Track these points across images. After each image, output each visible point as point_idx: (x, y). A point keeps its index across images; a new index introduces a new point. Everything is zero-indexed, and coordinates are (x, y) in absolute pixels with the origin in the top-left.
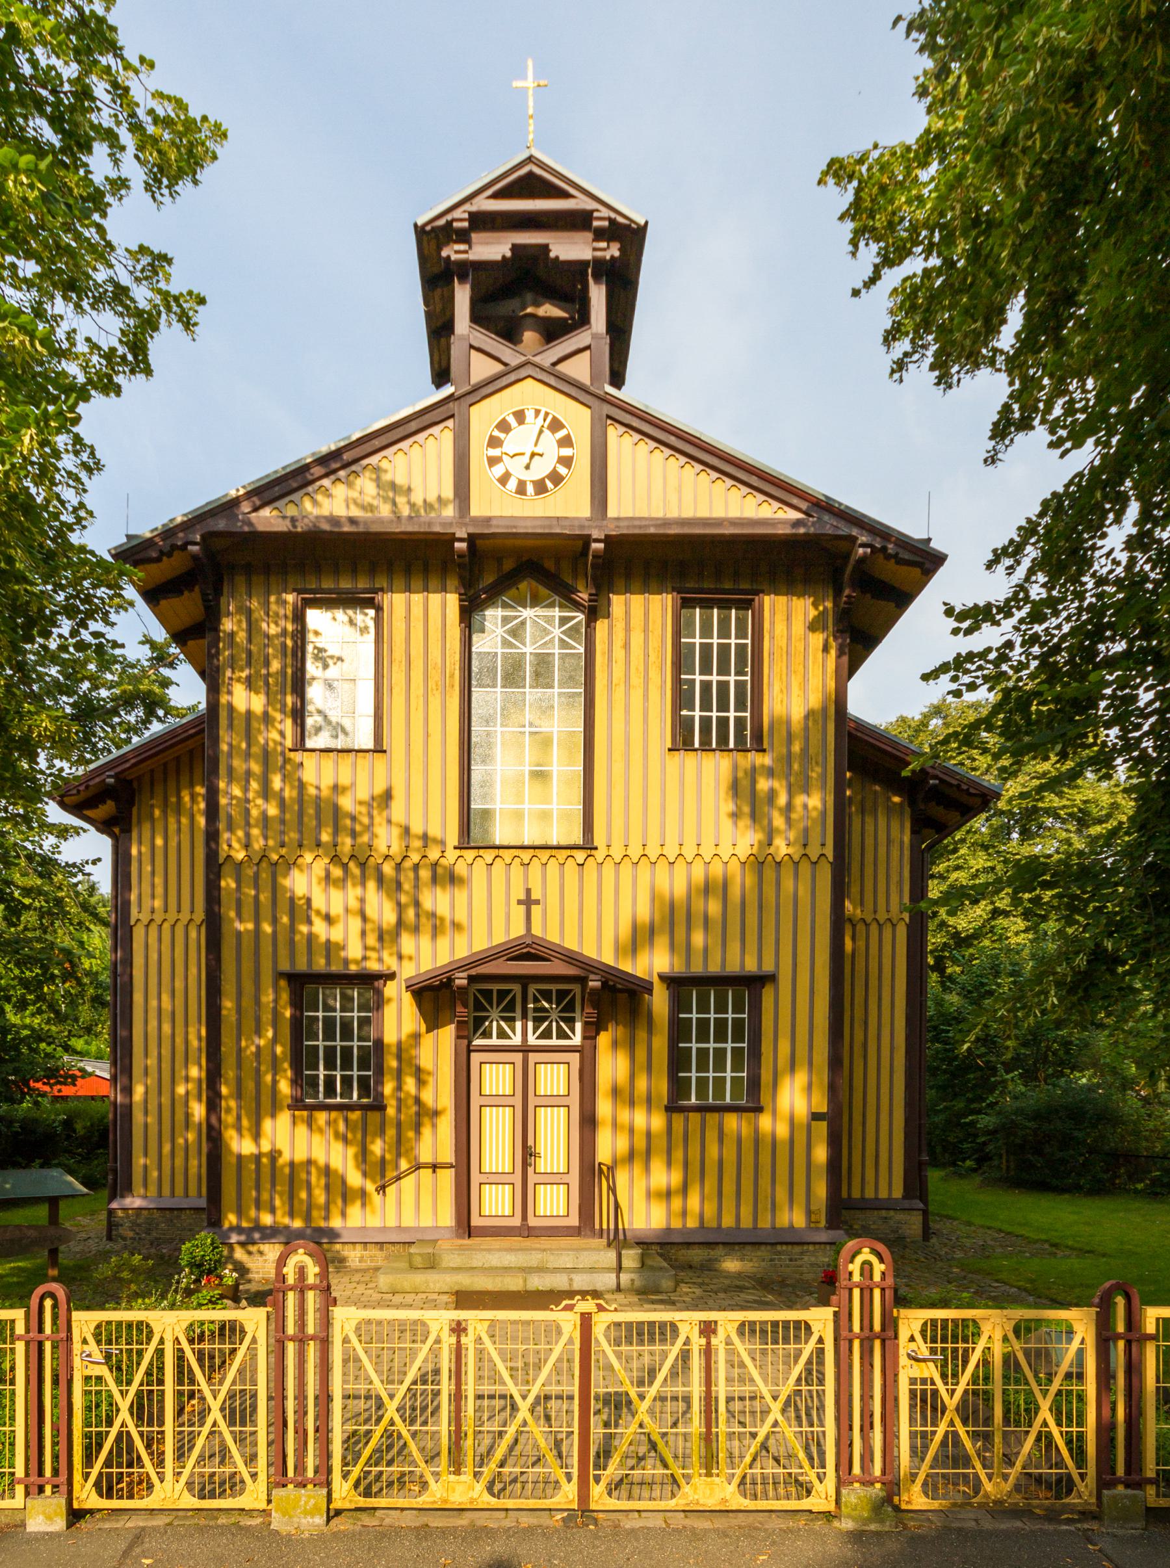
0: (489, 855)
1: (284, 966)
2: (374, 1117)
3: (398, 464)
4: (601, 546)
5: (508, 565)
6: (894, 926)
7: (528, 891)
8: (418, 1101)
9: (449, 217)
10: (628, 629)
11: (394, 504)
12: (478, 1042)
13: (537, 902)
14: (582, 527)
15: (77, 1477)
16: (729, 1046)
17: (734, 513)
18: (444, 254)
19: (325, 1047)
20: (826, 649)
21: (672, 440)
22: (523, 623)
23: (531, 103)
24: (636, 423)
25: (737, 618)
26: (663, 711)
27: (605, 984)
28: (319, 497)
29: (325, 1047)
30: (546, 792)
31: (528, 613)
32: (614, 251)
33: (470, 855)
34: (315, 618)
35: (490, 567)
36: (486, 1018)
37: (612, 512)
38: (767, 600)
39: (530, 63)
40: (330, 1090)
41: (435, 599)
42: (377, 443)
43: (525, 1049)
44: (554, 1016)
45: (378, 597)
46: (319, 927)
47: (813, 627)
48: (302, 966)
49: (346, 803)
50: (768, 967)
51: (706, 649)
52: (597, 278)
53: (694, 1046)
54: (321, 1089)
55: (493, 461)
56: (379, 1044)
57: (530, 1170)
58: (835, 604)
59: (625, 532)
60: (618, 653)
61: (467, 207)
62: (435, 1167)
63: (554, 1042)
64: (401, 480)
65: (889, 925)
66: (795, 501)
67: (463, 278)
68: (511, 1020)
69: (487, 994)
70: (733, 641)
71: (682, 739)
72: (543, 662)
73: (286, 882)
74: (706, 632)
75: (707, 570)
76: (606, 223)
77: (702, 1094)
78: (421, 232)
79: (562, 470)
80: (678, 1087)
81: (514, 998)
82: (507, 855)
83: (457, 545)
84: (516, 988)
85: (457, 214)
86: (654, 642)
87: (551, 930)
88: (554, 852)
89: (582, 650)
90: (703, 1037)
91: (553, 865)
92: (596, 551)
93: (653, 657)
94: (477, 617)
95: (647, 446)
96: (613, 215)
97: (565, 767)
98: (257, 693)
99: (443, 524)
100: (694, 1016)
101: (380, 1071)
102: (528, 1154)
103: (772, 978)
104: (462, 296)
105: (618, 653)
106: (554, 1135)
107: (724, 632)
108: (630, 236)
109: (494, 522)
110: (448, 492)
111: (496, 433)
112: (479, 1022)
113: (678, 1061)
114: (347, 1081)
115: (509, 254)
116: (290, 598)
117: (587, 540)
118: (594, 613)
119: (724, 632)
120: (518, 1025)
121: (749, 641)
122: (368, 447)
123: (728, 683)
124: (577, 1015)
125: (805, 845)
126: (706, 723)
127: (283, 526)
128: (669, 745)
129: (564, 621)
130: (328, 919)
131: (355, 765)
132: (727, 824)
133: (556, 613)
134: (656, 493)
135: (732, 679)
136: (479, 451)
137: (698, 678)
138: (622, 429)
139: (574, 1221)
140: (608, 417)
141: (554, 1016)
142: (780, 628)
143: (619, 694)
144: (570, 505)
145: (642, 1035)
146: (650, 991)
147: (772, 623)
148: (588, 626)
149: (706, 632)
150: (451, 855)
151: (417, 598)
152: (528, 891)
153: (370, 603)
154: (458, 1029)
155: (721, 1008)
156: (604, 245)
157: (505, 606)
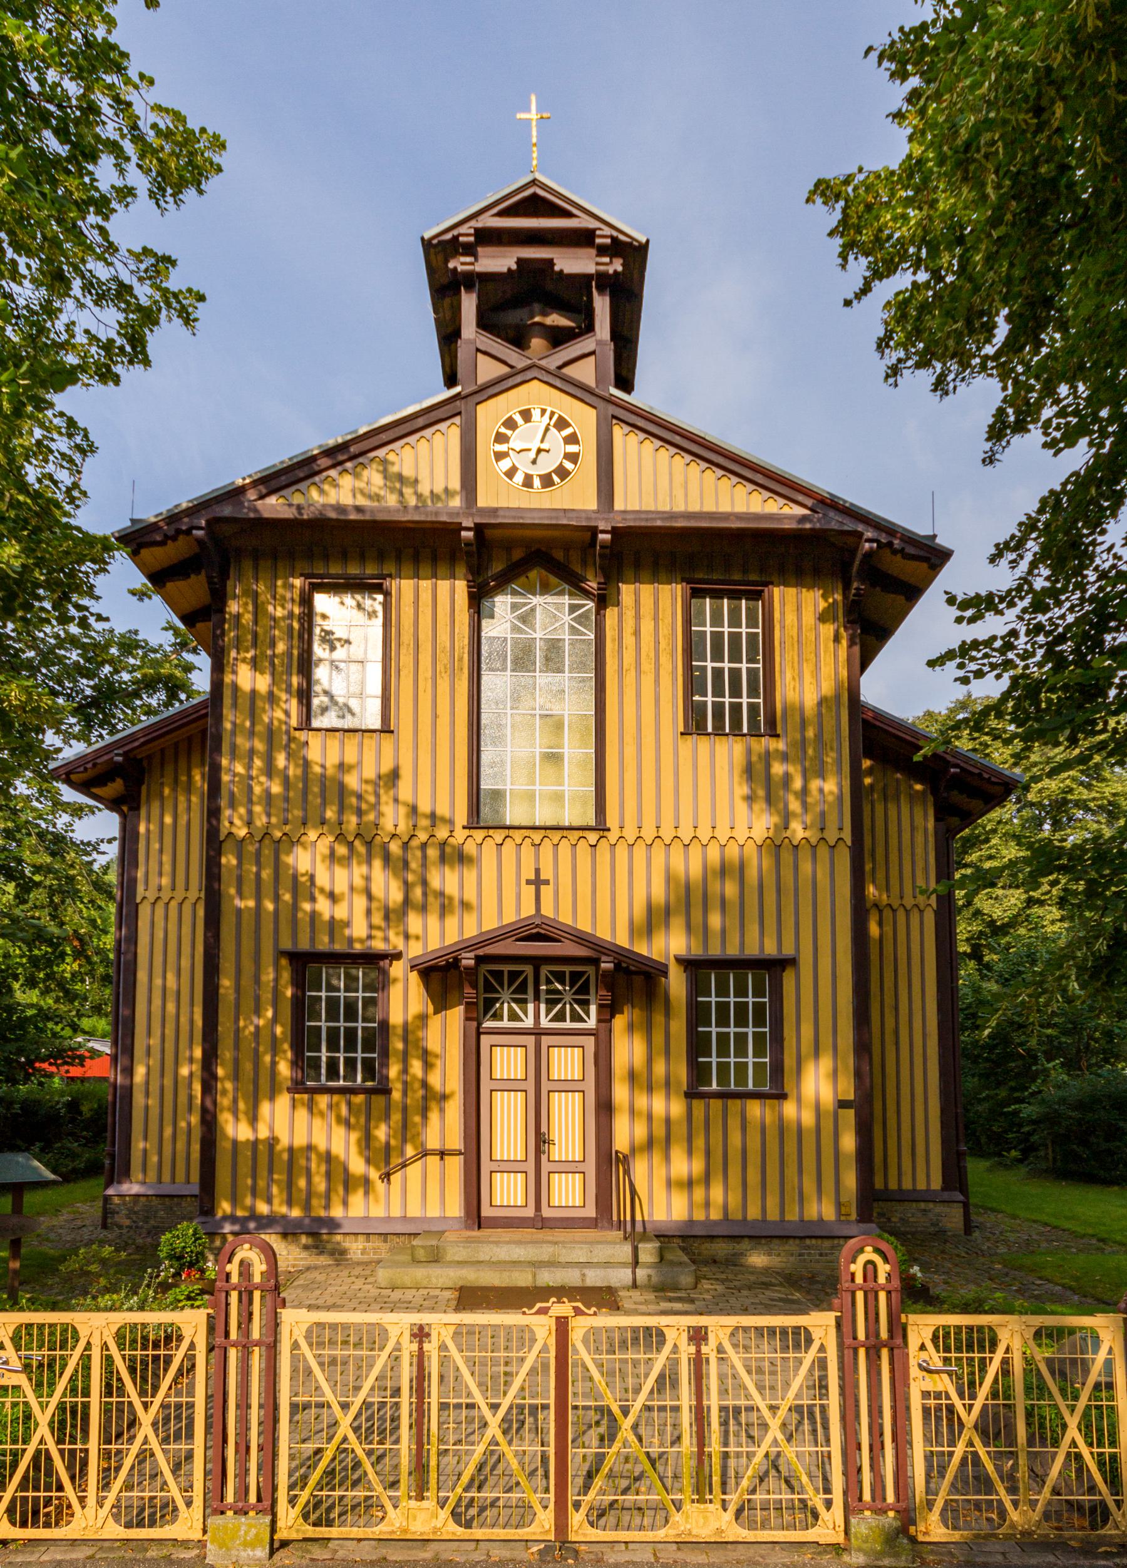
0: (498, 836)
1: (286, 944)
2: (378, 1101)
3: (405, 458)
4: (608, 537)
5: (518, 554)
6: (921, 911)
7: (537, 871)
8: (425, 1084)
9: (455, 232)
10: (638, 617)
11: (401, 494)
12: (488, 1024)
13: (547, 882)
14: (588, 519)
16: (750, 1030)
17: (740, 508)
18: (451, 265)
19: (328, 1028)
20: (837, 639)
21: (677, 439)
22: (533, 610)
23: (534, 133)
24: (641, 423)
25: (747, 609)
26: (675, 696)
27: (618, 966)
28: (326, 487)
29: (328, 1028)
30: (555, 769)
31: (536, 600)
32: (617, 266)
33: (479, 835)
34: (323, 602)
35: (498, 556)
36: (497, 999)
37: (618, 505)
38: (776, 591)
39: (533, 98)
40: (333, 1072)
41: (444, 585)
42: (384, 437)
43: (538, 1032)
44: (568, 998)
45: (387, 583)
46: (323, 906)
47: (822, 618)
48: (304, 945)
49: (352, 781)
50: (788, 951)
51: (717, 637)
52: (601, 289)
53: (714, 1030)
54: (323, 1071)
55: (500, 456)
56: (385, 1025)
57: (544, 1158)
58: (845, 596)
59: (632, 524)
60: (629, 640)
61: (473, 223)
62: (442, 1154)
63: (568, 1024)
64: (408, 472)
65: (916, 910)
66: (800, 498)
67: (469, 288)
68: (522, 1002)
69: (498, 975)
70: (744, 630)
71: (695, 723)
72: (553, 647)
73: (290, 860)
75: (715, 561)
76: (609, 241)
78: (427, 244)
79: (569, 466)
80: (698, 1073)
81: (526, 978)
82: (518, 835)
83: (464, 534)
84: (528, 969)
85: (463, 229)
86: (665, 630)
87: (560, 909)
88: (565, 833)
89: (593, 637)
91: (565, 847)
92: (603, 541)
93: (663, 644)
94: (486, 604)
95: (650, 445)
96: (615, 234)
97: (577, 751)
98: (262, 673)
99: (450, 514)
100: (713, 999)
101: (385, 1054)
102: (541, 1141)
104: (469, 304)
105: (629, 640)
106: (569, 1120)
107: (735, 621)
108: (635, 254)
109: (501, 513)
110: (455, 484)
111: (503, 430)
112: (489, 1004)
113: (697, 1046)
114: (351, 1063)
115: (514, 267)
116: (297, 582)
117: (594, 531)
118: (602, 602)
119: (735, 621)
120: (531, 1007)
121: (760, 631)
122: (374, 441)
123: (740, 670)
124: (592, 997)
125: (822, 829)
126: (718, 708)
127: (289, 514)
128: (681, 729)
129: (573, 608)
130: (332, 897)
131: (361, 745)
132: (742, 807)
133: (566, 600)
135: (744, 666)
136: (485, 446)
137: (709, 665)
138: (627, 429)
139: (591, 1212)
140: (614, 417)
141: (568, 998)
142: (791, 618)
143: (630, 678)
144: (577, 498)
145: (659, 1019)
146: (665, 974)
147: (783, 614)
148: (598, 613)
149: (717, 620)
150: (460, 835)
151: (425, 584)
152: (537, 871)
153: (378, 588)
154: (466, 1011)
155: (741, 991)
156: (606, 260)
157: (514, 593)
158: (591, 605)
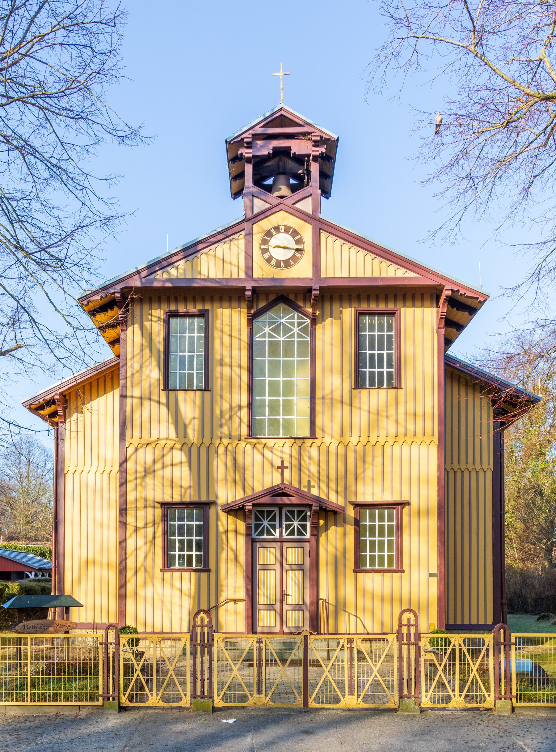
9: (242, 136)
13: (287, 467)
15: (122, 695)
16: (386, 539)
18: (240, 152)
25: (388, 322)
50: (405, 498)
61: (251, 132)
69: (262, 512)
74: (372, 329)
76: (318, 138)
84: (277, 510)
108: (331, 144)
128: (353, 387)
129: (299, 324)
134: (344, 264)
135: (385, 352)
158: (308, 321)
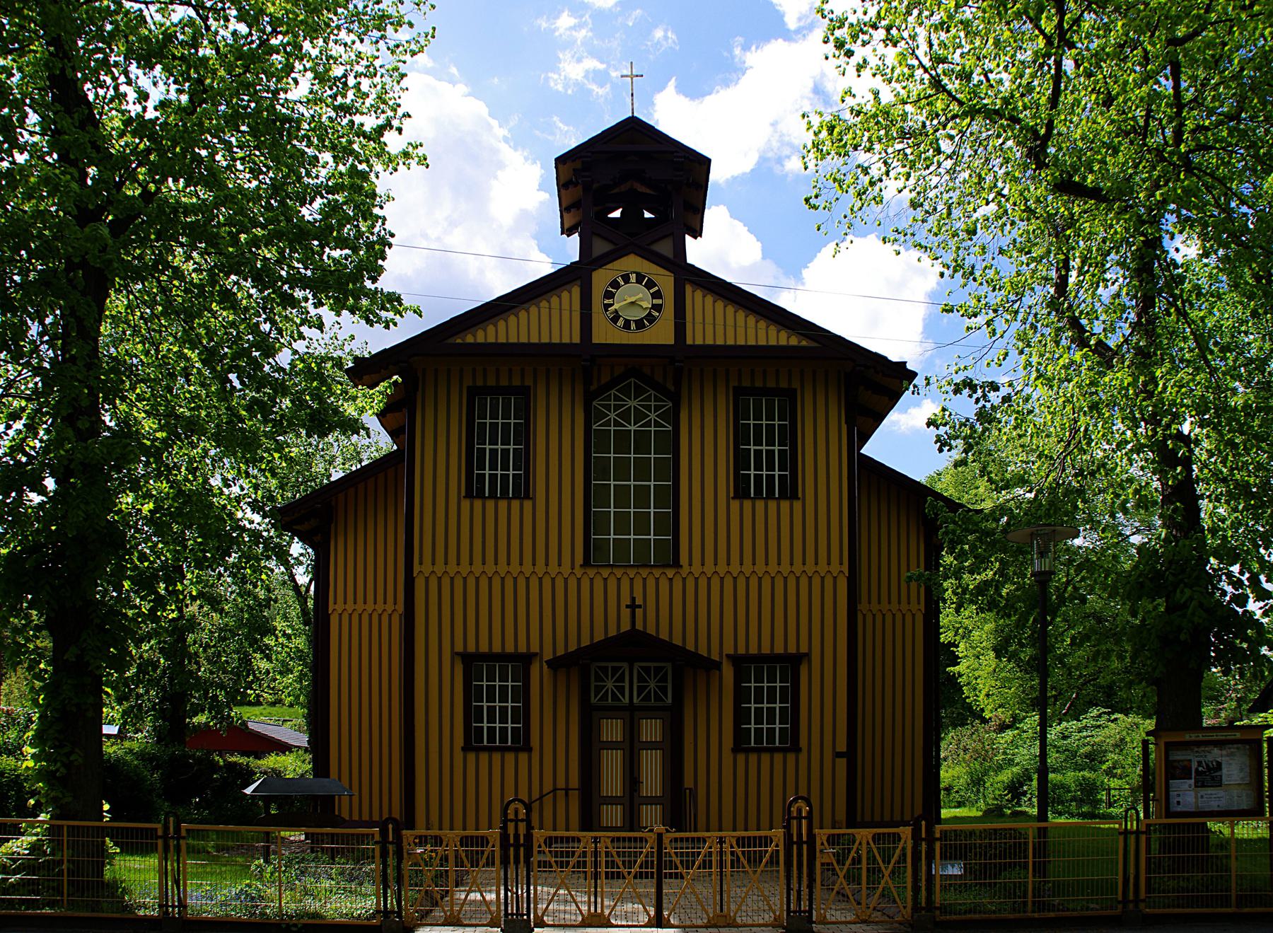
0: (605, 572)
13: (639, 606)
33: (591, 572)
50: (804, 649)
53: (753, 706)
77: (759, 739)
90: (759, 700)
103: (808, 655)
106: (652, 768)
126: (758, 478)
144: (662, 334)
152: (633, 599)
